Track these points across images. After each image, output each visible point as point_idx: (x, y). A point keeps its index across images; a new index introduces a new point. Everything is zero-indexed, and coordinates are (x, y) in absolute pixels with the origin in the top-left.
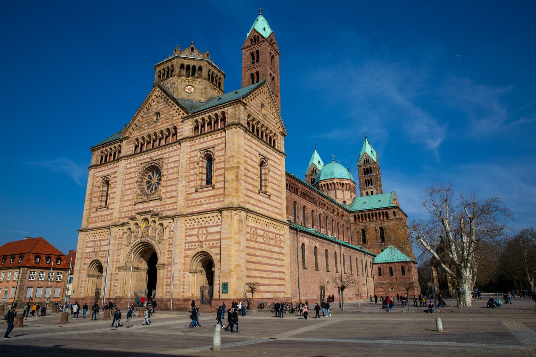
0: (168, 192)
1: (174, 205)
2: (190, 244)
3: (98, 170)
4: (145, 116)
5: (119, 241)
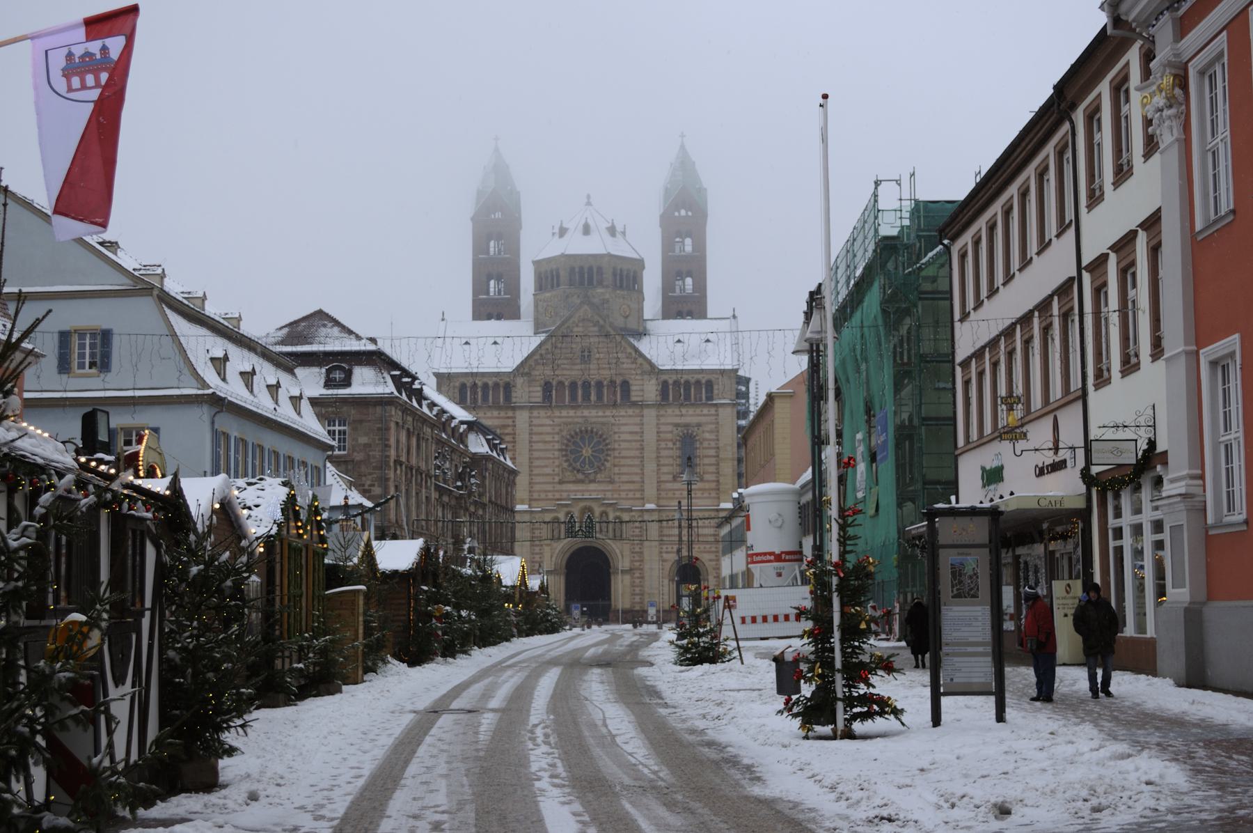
0: (623, 474)
1: (637, 493)
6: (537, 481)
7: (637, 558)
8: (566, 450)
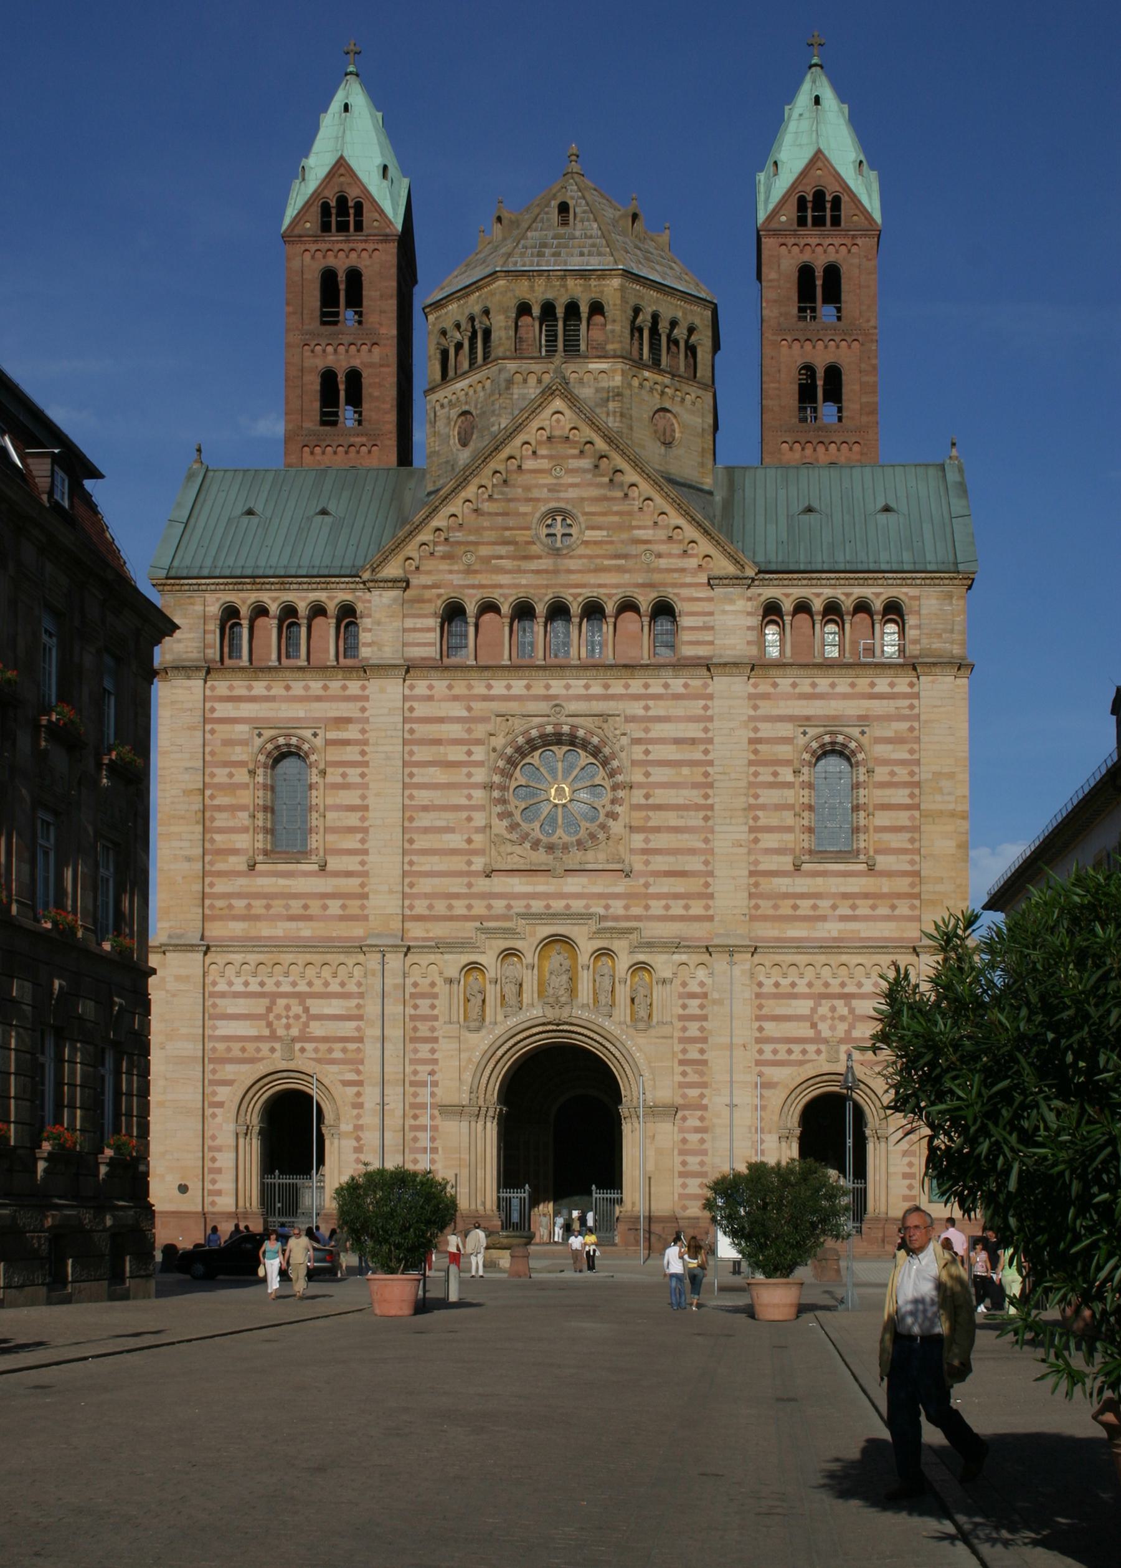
1: (691, 902)
2: (782, 1048)
3: (221, 686)
4: (486, 507)
5: (416, 1007)
6: (427, 868)
7: (693, 1078)
8: (503, 788)
